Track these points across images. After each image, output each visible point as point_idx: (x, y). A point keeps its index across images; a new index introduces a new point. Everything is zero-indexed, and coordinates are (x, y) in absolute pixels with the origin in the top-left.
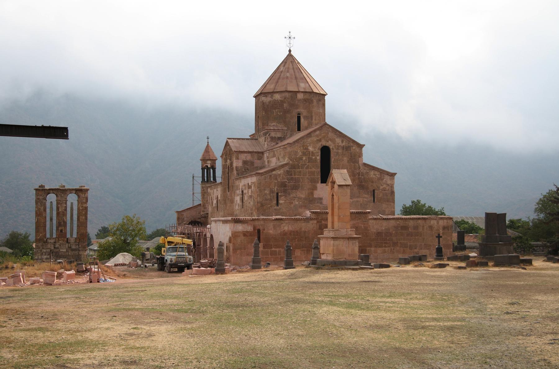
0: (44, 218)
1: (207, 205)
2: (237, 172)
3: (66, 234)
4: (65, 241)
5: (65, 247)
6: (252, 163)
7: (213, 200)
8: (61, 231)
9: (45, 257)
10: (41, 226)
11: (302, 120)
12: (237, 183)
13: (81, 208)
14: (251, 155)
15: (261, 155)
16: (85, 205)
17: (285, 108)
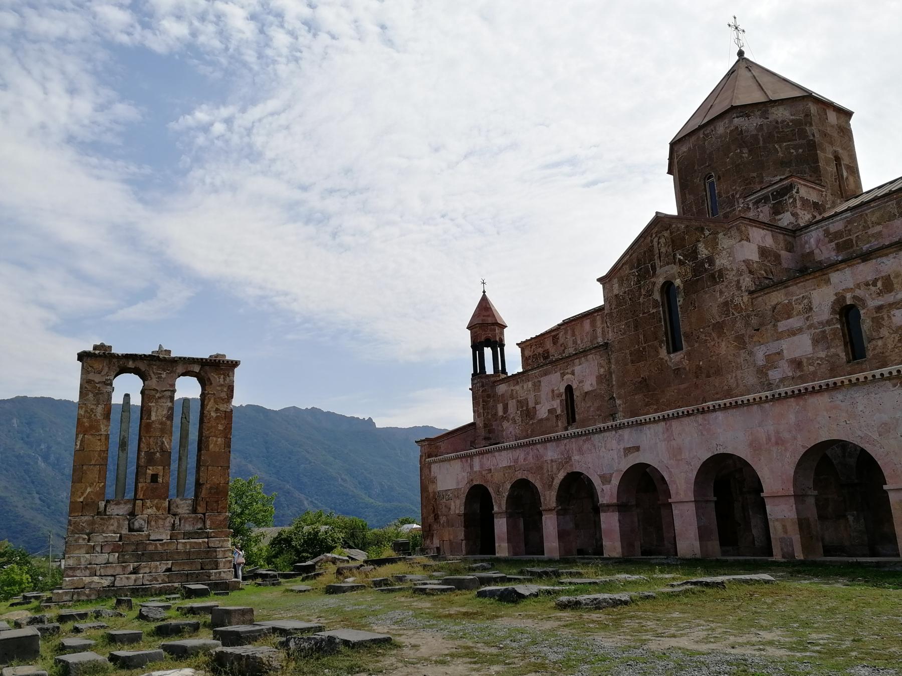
0: (103, 438)
1: (494, 423)
2: (752, 276)
3: (167, 486)
4: (165, 508)
5: (164, 526)
6: (778, 257)
7: (537, 403)
8: (154, 478)
9: (102, 558)
10: (93, 462)
11: (845, 174)
12: (777, 297)
13: (213, 414)
14: (773, 236)
15: (790, 239)
16: (222, 407)
17: (812, 138)
